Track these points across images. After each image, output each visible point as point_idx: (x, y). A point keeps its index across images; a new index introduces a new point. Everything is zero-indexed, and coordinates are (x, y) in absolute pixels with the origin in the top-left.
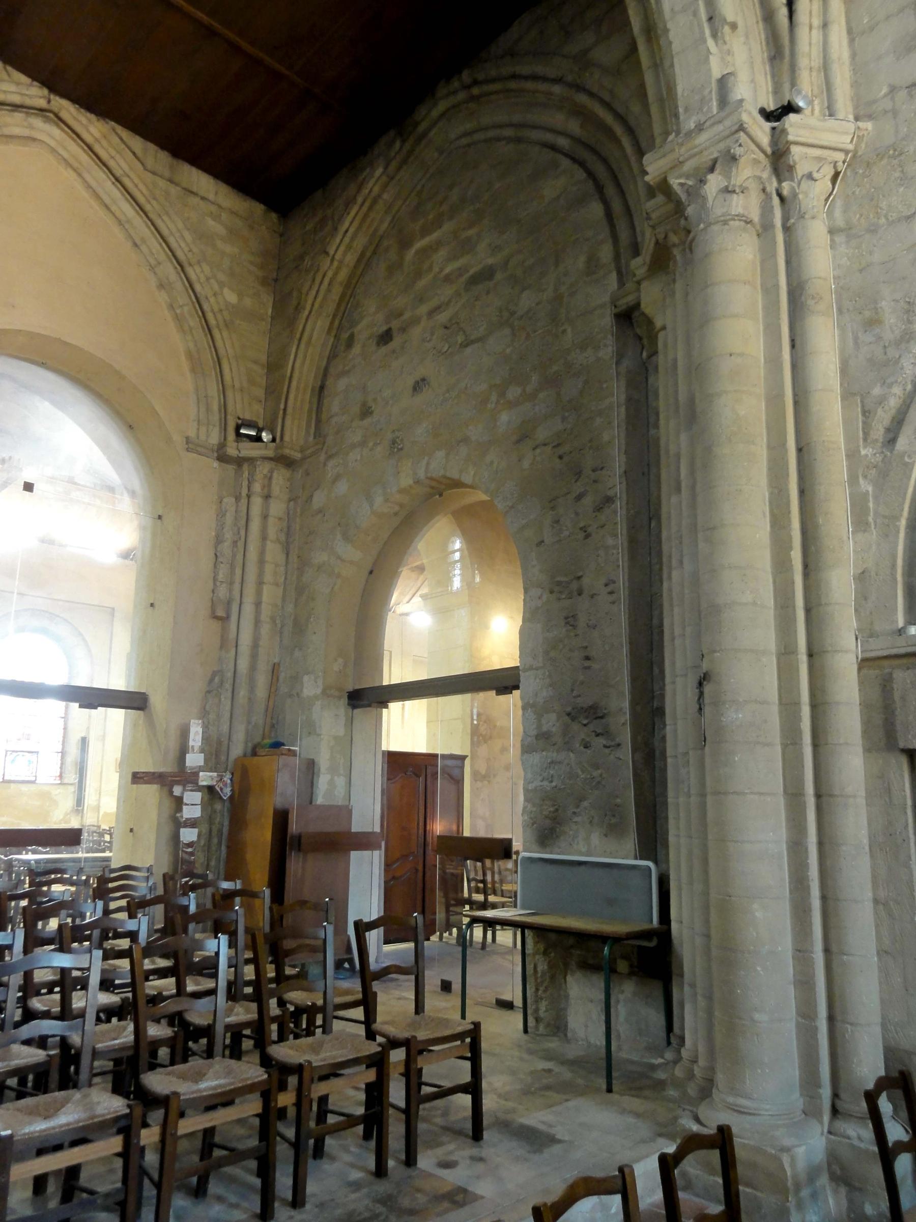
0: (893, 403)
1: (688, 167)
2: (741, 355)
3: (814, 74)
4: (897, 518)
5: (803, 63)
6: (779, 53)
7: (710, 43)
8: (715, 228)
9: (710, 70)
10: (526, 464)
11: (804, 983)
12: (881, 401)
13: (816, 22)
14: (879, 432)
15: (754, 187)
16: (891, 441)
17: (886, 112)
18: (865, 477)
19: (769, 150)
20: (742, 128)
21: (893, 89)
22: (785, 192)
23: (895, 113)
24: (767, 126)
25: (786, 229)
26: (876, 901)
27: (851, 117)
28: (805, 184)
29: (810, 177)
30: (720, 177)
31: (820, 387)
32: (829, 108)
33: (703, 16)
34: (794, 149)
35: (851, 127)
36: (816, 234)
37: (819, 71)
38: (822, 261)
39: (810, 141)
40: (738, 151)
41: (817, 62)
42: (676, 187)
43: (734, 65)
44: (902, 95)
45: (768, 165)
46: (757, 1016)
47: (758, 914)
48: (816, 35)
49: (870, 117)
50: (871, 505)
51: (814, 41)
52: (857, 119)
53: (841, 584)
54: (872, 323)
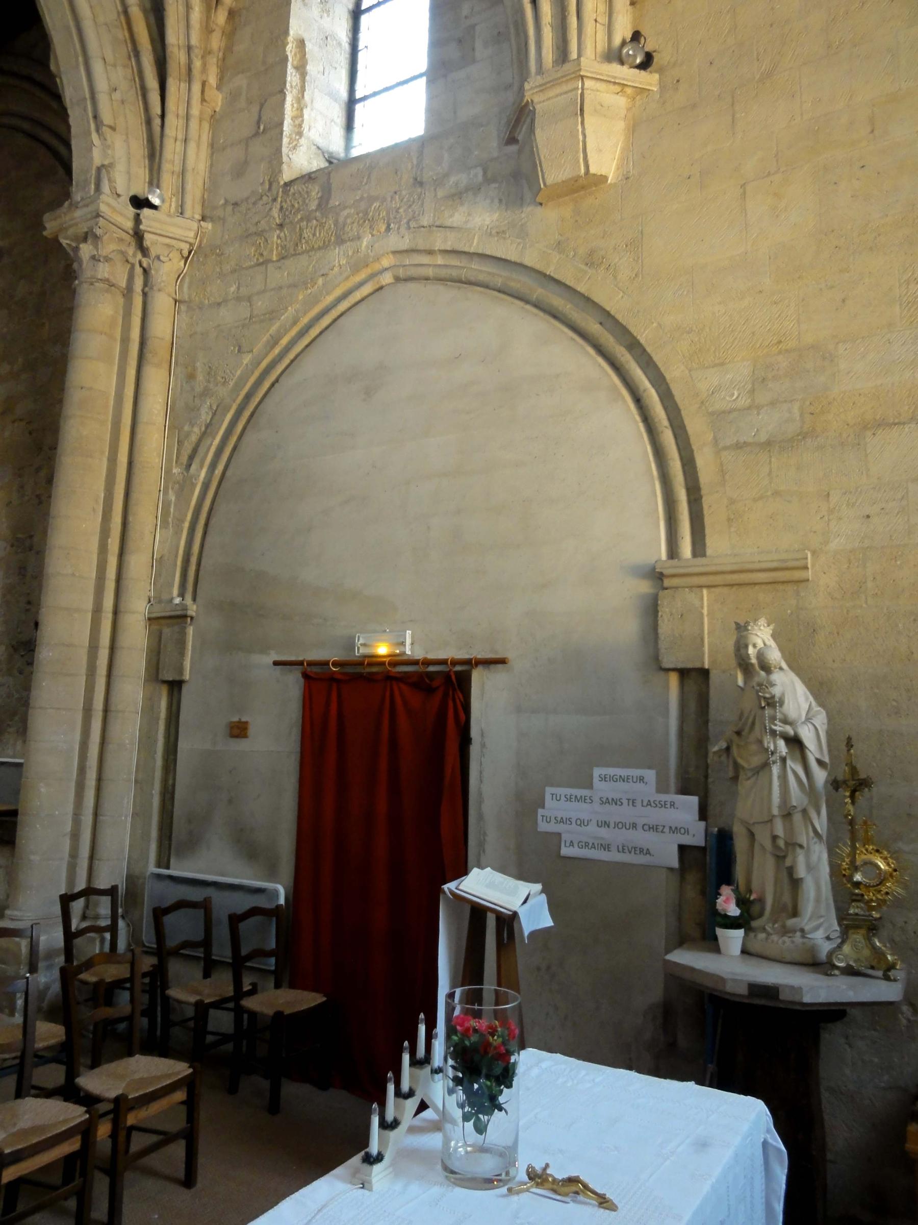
0: (194, 438)
1: (71, 232)
2: (91, 389)
3: (175, 177)
4: (183, 521)
5: (166, 167)
6: (154, 154)
7: (94, 136)
8: (85, 286)
9: (92, 158)
10: (7, 434)
11: (75, 836)
12: (188, 435)
13: (181, 136)
14: (184, 459)
15: (117, 258)
16: (189, 466)
17: (219, 218)
18: (172, 488)
19: (131, 232)
20: (98, 215)
21: (226, 201)
22: (145, 265)
23: (224, 220)
24: (131, 211)
25: (145, 294)
26: (136, 781)
27: (198, 217)
28: (156, 263)
29: (158, 258)
30: (91, 247)
31: (145, 420)
32: (182, 206)
33: (90, 115)
34: (146, 236)
35: (195, 225)
36: (162, 303)
37: (178, 176)
38: (162, 325)
39: (158, 232)
40: (98, 232)
41: (178, 168)
42: (64, 245)
43: (113, 157)
44: (229, 208)
45: (133, 244)
46: (32, 857)
47: (42, 790)
48: (179, 147)
49: (212, 220)
50: (172, 510)
51: (178, 149)
52: (203, 219)
53: (139, 565)
54: (191, 377)
